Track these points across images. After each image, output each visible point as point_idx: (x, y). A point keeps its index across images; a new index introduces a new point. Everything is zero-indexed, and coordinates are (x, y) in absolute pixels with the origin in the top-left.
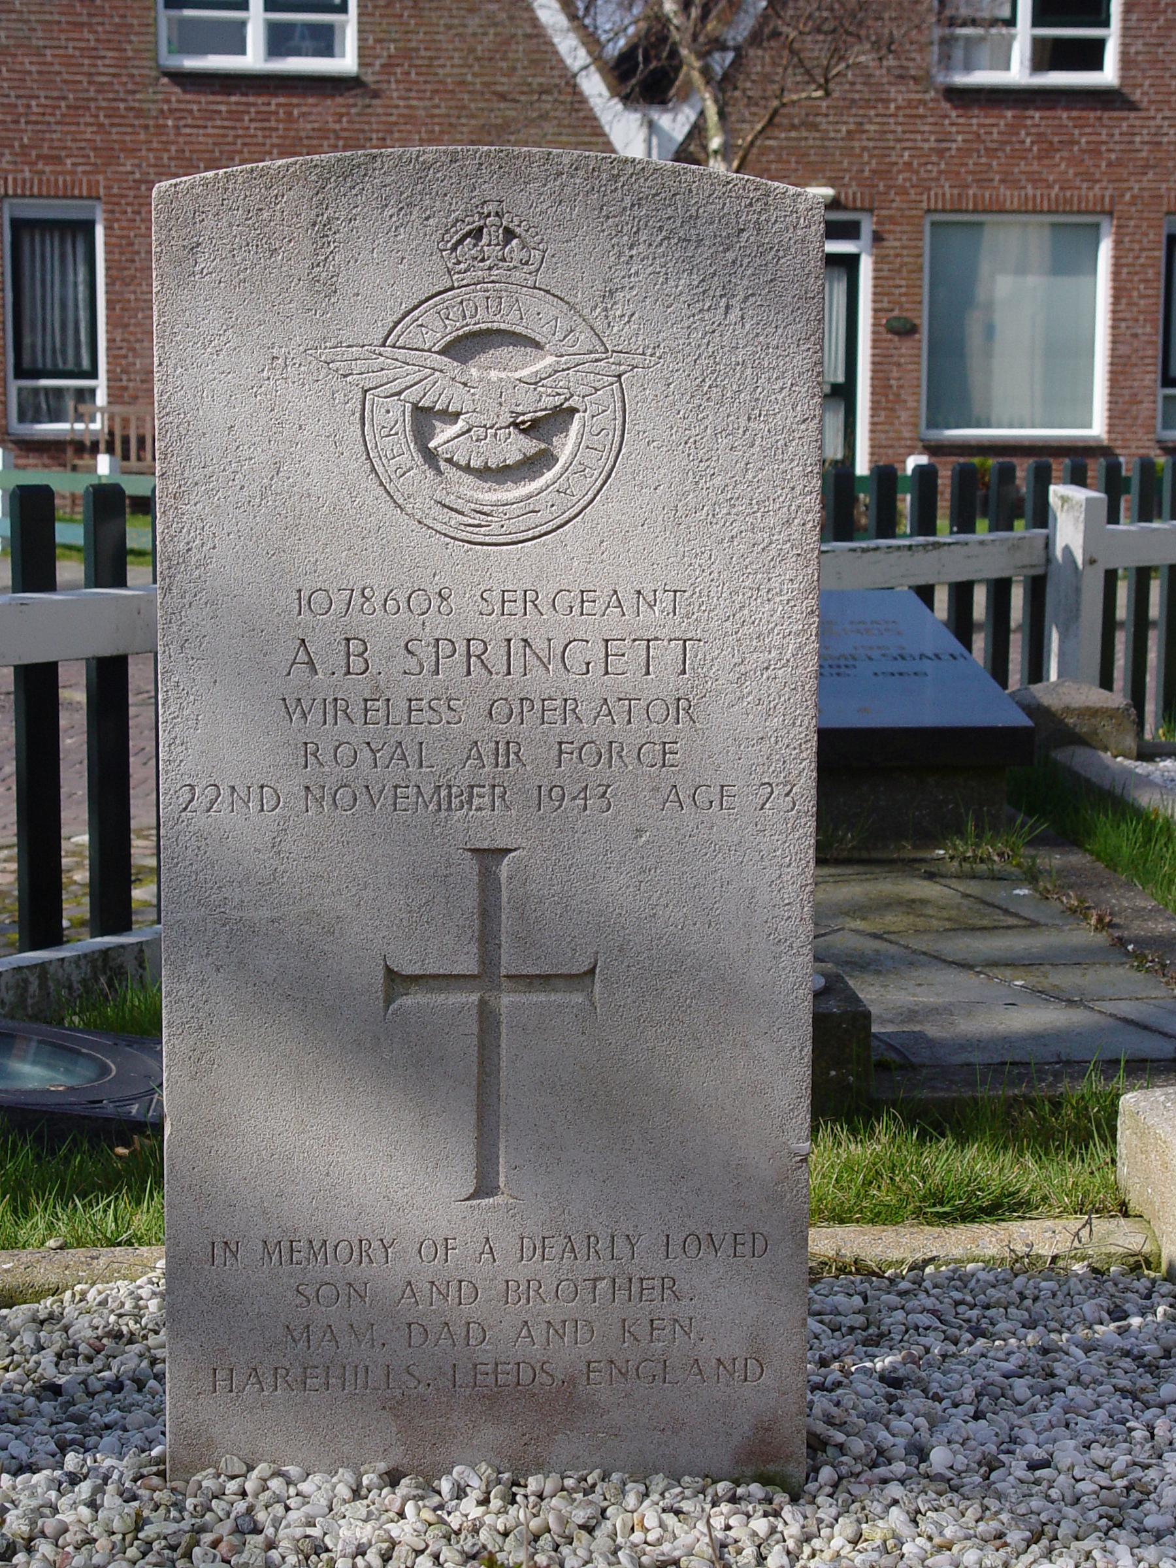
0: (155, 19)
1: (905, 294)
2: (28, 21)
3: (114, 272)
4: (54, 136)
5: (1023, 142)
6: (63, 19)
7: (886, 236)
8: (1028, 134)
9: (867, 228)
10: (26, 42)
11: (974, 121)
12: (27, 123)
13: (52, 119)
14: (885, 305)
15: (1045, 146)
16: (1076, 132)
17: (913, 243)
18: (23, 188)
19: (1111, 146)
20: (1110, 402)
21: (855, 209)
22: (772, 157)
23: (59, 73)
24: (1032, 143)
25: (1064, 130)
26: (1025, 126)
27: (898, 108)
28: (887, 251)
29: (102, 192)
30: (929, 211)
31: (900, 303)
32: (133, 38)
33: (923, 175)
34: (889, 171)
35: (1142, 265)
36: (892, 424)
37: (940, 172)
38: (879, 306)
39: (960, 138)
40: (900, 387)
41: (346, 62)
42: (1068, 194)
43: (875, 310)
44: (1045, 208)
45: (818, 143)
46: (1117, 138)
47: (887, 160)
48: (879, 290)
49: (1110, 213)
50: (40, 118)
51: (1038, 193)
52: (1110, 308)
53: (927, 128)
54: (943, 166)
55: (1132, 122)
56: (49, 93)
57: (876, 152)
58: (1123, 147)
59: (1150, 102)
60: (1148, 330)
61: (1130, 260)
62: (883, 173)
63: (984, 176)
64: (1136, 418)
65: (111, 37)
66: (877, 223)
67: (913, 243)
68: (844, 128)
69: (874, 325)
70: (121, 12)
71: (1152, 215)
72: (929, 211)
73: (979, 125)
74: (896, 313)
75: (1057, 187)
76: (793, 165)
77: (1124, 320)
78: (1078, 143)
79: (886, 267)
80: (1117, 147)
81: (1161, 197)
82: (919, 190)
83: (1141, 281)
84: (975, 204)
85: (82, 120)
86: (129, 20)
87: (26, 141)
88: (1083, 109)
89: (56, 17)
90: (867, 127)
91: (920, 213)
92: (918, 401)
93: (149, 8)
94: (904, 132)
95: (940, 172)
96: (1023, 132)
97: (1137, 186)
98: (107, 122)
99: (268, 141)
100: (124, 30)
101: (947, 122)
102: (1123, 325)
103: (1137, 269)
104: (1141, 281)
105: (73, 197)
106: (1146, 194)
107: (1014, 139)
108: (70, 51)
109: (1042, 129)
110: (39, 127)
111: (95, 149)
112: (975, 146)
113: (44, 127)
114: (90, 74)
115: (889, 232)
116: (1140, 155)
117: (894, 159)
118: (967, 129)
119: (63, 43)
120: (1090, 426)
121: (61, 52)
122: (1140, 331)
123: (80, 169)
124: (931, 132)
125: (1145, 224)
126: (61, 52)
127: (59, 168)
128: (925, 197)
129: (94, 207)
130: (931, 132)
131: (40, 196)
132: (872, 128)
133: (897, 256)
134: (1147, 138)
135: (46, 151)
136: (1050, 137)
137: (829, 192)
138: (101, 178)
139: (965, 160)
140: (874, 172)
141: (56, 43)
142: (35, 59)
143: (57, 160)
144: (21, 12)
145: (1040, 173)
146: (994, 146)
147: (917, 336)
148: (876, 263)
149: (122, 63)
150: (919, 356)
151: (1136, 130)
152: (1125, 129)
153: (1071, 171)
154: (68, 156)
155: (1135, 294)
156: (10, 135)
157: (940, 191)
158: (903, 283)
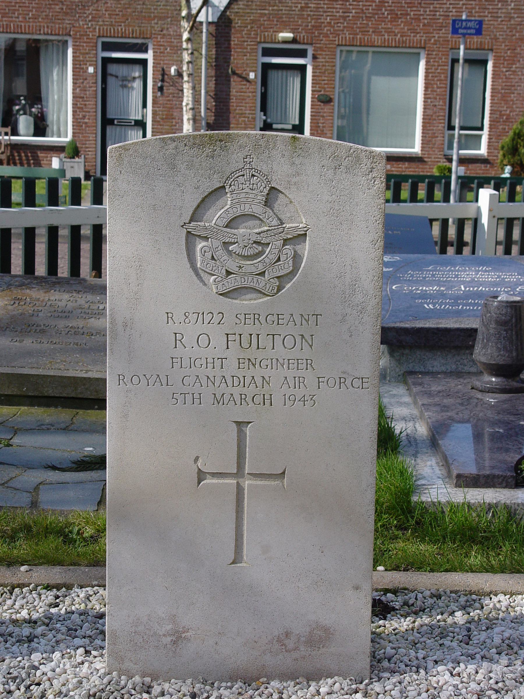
1: (326, 84)
5: (384, 14)
7: (318, 56)
8: (386, 10)
9: (310, 53)
11: (361, 3)
14: (317, 89)
15: (394, 16)
16: (409, 9)
17: (331, 60)
19: (425, 17)
20: (422, 137)
21: (304, 43)
22: (265, 18)
24: (388, 14)
25: (403, 9)
26: (385, 6)
28: (318, 64)
31: (324, 88)
33: (337, 28)
34: (321, 26)
37: (344, 27)
38: (314, 89)
39: (354, 11)
40: (323, 127)
42: (404, 39)
43: (313, 91)
44: (394, 45)
45: (286, 12)
46: (428, 13)
47: (319, 21)
48: (314, 82)
49: (424, 48)
51: (390, 38)
52: (423, 92)
53: (338, 6)
54: (345, 24)
55: (435, 5)
57: (315, 17)
58: (431, 17)
60: (441, 103)
61: (433, 70)
63: (364, 29)
64: (435, 144)
66: (314, 50)
67: (331, 60)
68: (299, 6)
69: (312, 98)
71: (444, 50)
72: (338, 45)
73: (363, 6)
74: (322, 93)
75: (399, 35)
76: (275, 22)
78: (410, 15)
79: (318, 71)
80: (428, 17)
81: (448, 41)
82: (334, 35)
83: (438, 80)
84: (361, 43)
90: (310, 5)
91: (335, 46)
94: (328, 8)
95: (344, 27)
96: (384, 9)
97: (437, 36)
99: (31, 6)
101: (348, 4)
102: (429, 100)
103: (437, 74)
104: (438, 80)
106: (441, 39)
107: (379, 12)
109: (393, 8)
112: (361, 15)
115: (320, 54)
116: (438, 21)
117: (322, 21)
118: (357, 7)
120: (414, 148)
122: (437, 104)
124: (340, 8)
125: (440, 53)
128: (337, 39)
130: (340, 8)
132: (312, 6)
133: (323, 66)
134: (442, 13)
136: (396, 12)
139: (356, 22)
140: (313, 26)
145: (392, 28)
146: (370, 15)
147: (332, 104)
148: (313, 69)
150: (332, 113)
151: (437, 9)
152: (432, 9)
153: (406, 28)
155: (435, 86)
157: (344, 36)
158: (326, 78)
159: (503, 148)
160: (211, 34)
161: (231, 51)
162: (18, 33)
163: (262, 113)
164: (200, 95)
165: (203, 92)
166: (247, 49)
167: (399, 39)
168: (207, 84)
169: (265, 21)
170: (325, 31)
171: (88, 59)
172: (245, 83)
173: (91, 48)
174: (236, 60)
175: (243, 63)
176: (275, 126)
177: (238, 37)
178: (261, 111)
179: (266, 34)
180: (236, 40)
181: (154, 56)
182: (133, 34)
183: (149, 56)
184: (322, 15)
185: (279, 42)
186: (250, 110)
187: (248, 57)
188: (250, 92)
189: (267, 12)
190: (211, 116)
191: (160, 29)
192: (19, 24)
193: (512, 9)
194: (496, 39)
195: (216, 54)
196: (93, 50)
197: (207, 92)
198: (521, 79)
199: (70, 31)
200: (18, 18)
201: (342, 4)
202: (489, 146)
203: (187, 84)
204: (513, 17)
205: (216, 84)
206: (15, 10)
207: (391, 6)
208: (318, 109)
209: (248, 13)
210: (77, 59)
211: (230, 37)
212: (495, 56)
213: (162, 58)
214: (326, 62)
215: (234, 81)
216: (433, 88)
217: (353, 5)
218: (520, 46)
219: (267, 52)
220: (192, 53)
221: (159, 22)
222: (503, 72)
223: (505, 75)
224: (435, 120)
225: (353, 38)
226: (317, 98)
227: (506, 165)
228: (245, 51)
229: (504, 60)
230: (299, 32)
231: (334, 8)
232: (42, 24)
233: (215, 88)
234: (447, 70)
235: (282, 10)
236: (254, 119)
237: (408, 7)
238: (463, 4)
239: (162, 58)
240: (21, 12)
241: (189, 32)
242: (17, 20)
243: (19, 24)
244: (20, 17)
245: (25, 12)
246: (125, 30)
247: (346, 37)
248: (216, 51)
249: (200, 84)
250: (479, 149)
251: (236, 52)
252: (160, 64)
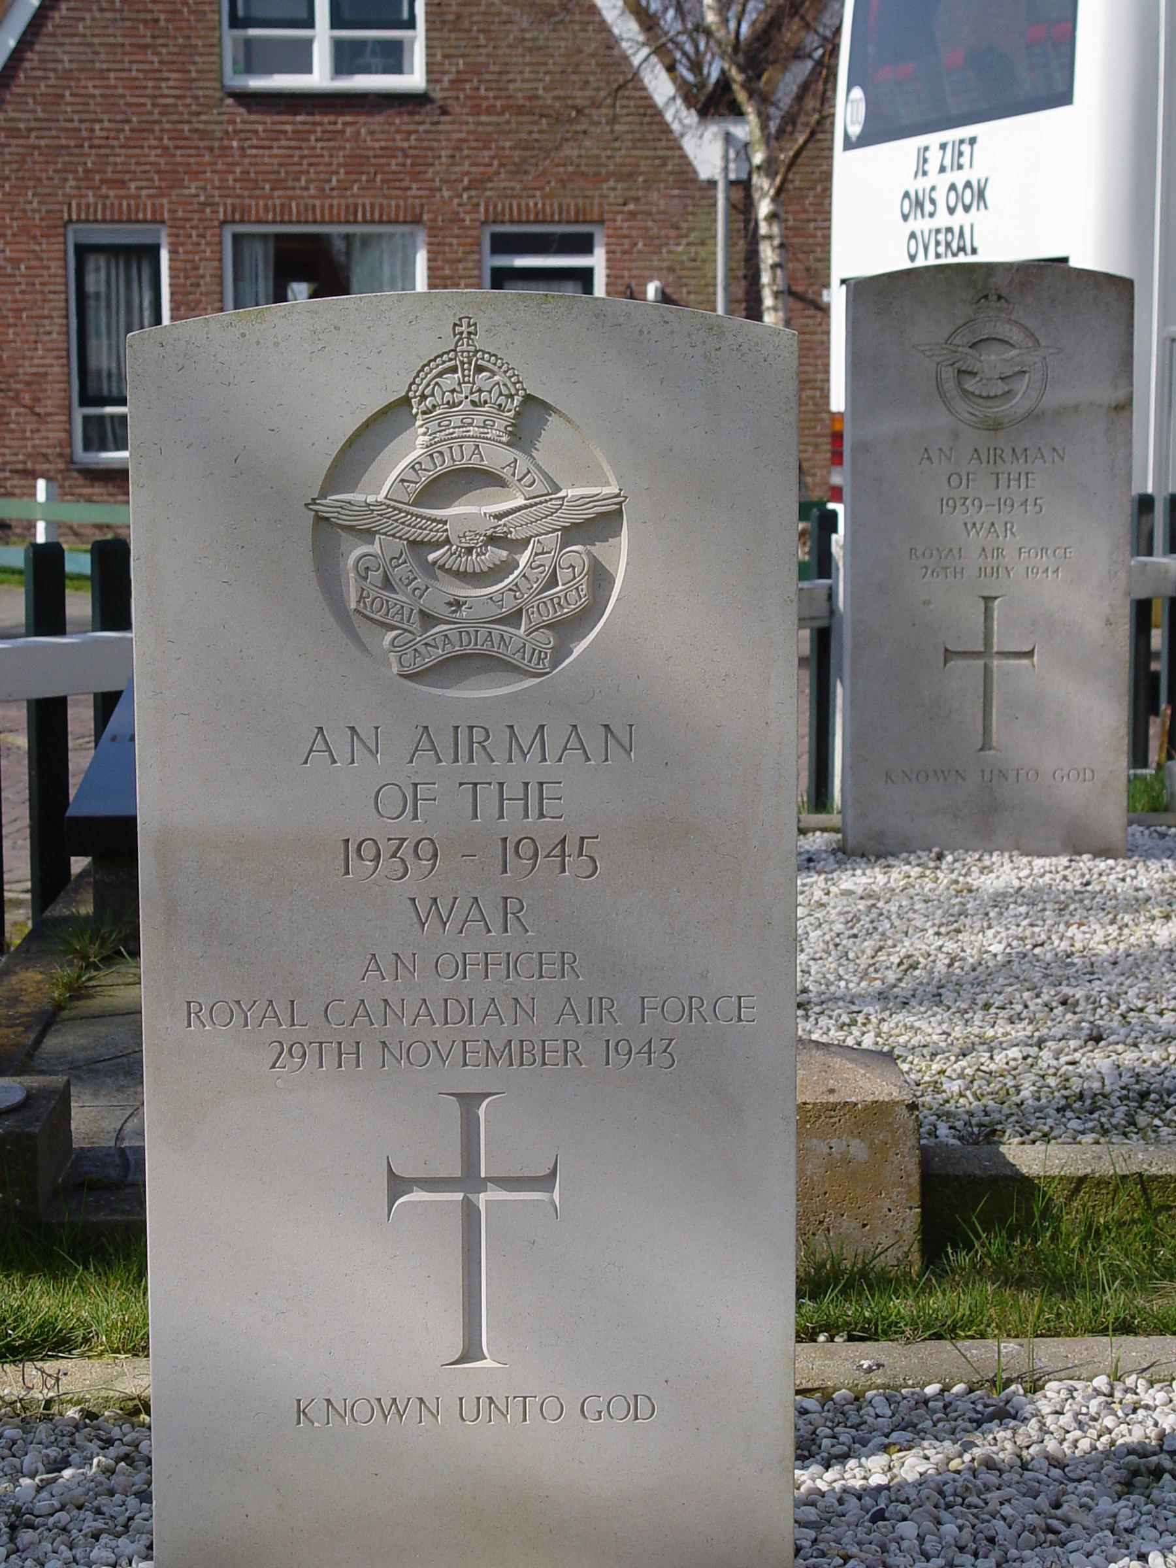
0: (220, 39)
2: (90, 45)
3: (179, 297)
4: (118, 160)
6: (127, 41)
10: (90, 65)
12: (91, 147)
13: (116, 143)
18: (87, 213)
23: (122, 96)
29: (166, 215)
32: (198, 59)
41: (414, 79)
50: (103, 142)
56: (113, 117)
65: (175, 58)
70: (186, 33)
85: (146, 144)
86: (194, 41)
87: (89, 165)
89: (120, 40)
93: (213, 29)
98: (171, 144)
100: (187, 51)
105: (138, 221)
108: (134, 74)
110: (103, 151)
111: (159, 172)
113: (108, 151)
114: (154, 97)
119: (127, 65)
121: (125, 75)
123: (144, 192)
126: (125, 75)
127: (123, 192)
129: (159, 231)
131: (104, 221)
135: (109, 175)
138: (165, 201)
141: (119, 66)
142: (97, 82)
143: (122, 184)
144: (85, 36)
149: (187, 84)
154: (131, 180)
156: (75, 159)
162: (306, 222)
166: (814, 236)
171: (461, 272)
172: (811, 312)
173: (467, 248)
177: (795, 213)
180: (790, 217)
181: (608, 260)
182: (560, 214)
183: (597, 261)
191: (621, 201)
192: (310, 202)
196: (473, 252)
199: (421, 214)
200: (306, 189)
203: (772, 313)
206: (301, 172)
210: (438, 273)
213: (627, 264)
220: (782, 246)
221: (619, 186)
228: (811, 241)
232: (360, 201)
239: (627, 264)
240: (313, 176)
241: (774, 200)
242: (305, 194)
243: (310, 202)
244: (312, 186)
245: (322, 176)
246: (544, 205)
252: (622, 277)
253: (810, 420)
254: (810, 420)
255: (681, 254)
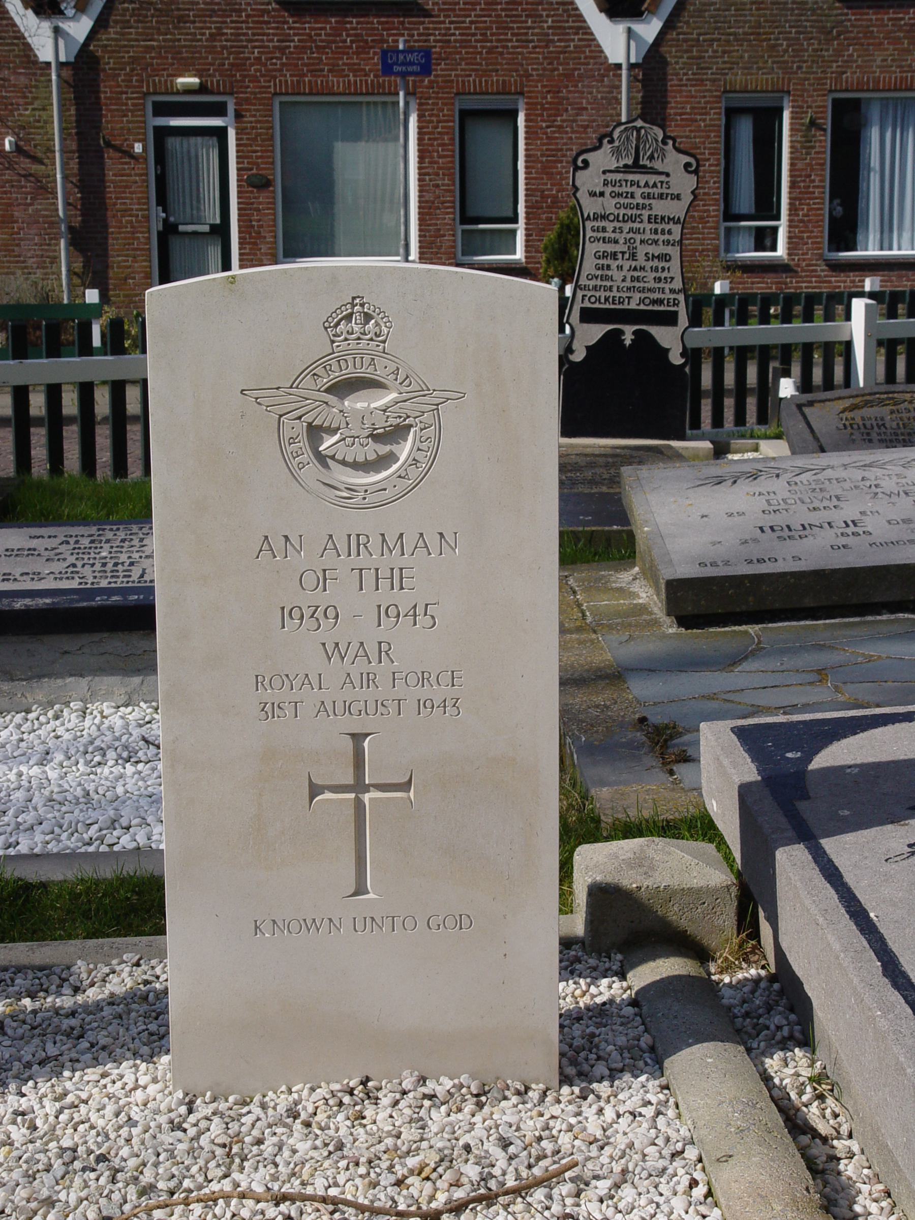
5: (345, 41)
8: (348, 35)
9: (231, 108)
14: (246, 165)
21: (219, 93)
26: (346, 29)
27: (248, 16)
30: (275, 94)
31: (257, 164)
34: (245, 64)
35: (439, 133)
36: (255, 254)
37: (283, 64)
39: (296, 39)
43: (238, 169)
46: (416, 38)
59: (439, 10)
62: (239, 66)
72: (275, 94)
73: (311, 29)
74: (254, 171)
77: (428, 174)
83: (439, 145)
84: (311, 88)
88: (389, 16)
92: (275, 237)
94: (254, 35)
95: (283, 64)
102: (427, 178)
104: (439, 145)
115: (247, 110)
130: (273, 34)
133: (253, 128)
137: (196, 80)
140: (232, 65)
145: (359, 64)
148: (237, 134)
150: (274, 203)
159: (546, 248)
160: (66, 82)
161: (101, 110)
163: (160, 208)
164: (55, 181)
165: (59, 176)
166: (127, 104)
167: (372, 81)
168: (64, 165)
169: (152, 58)
170: (252, 72)
172: (127, 160)
174: (112, 123)
175: (122, 128)
176: (182, 228)
177: (110, 87)
178: (158, 205)
179: (157, 79)
184: (246, 47)
185: (178, 93)
186: (139, 204)
187: (130, 118)
188: (136, 175)
189: (155, 43)
190: (76, 216)
193: (549, 28)
194: (528, 76)
195: (76, 115)
197: (65, 178)
198: (571, 138)
201: (277, 28)
202: (526, 246)
204: (552, 41)
205: (80, 163)
207: (355, 29)
208: (249, 198)
209: (125, 46)
211: (99, 86)
212: (527, 103)
214: (256, 122)
215: (109, 158)
216: (432, 157)
217: (294, 28)
218: (567, 87)
219: (162, 109)
222: (541, 128)
223: (546, 133)
224: (438, 208)
225: (298, 82)
226: (246, 181)
227: (553, 277)
229: (543, 109)
230: (210, 76)
231: (264, 34)
233: (79, 170)
234: (453, 128)
235: (179, 40)
236: (147, 218)
237: (383, 29)
238: (471, 22)
247: (286, 81)
248: (77, 110)
249: (54, 164)
250: (515, 253)
251: (110, 110)
253: (129, 238)
254: (129, 238)
255: (28, 116)
